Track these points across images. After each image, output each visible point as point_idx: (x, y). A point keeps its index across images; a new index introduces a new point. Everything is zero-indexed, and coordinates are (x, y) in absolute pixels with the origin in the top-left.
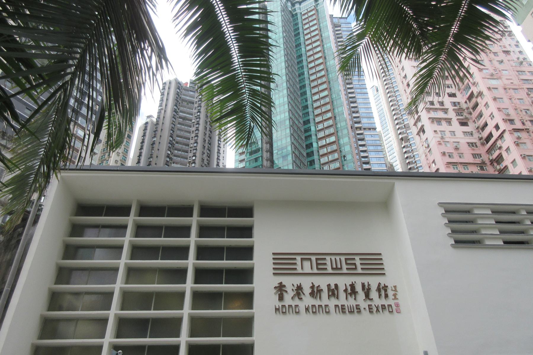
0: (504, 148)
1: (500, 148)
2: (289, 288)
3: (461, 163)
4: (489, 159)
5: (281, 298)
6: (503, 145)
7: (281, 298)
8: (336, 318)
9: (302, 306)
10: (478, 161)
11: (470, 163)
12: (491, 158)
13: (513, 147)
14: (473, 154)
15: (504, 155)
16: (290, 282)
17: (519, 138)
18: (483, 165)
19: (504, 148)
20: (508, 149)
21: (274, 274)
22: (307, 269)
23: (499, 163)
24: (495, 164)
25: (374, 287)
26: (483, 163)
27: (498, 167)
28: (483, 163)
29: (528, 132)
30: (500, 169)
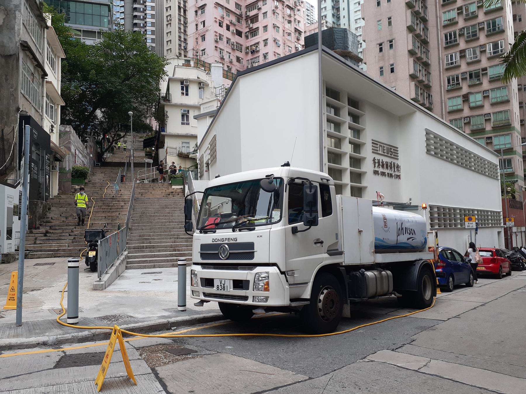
0: (263, 11)
1: (259, 9)
2: (376, 161)
3: (226, 8)
4: (246, 14)
5: (375, 166)
6: (263, 8)
7: (375, 166)
8: (386, 179)
9: (380, 172)
10: (238, 12)
11: (232, 11)
12: (248, 14)
13: (270, 14)
14: (236, 3)
15: (261, 17)
16: (377, 157)
17: (276, 7)
18: (241, 18)
19: (263, 11)
20: (265, 13)
21: (373, 152)
22: (380, 152)
23: (252, 22)
24: (249, 22)
25: (396, 165)
26: (241, 16)
27: (251, 26)
28: (241, 16)
29: (283, 5)
30: (252, 28)
